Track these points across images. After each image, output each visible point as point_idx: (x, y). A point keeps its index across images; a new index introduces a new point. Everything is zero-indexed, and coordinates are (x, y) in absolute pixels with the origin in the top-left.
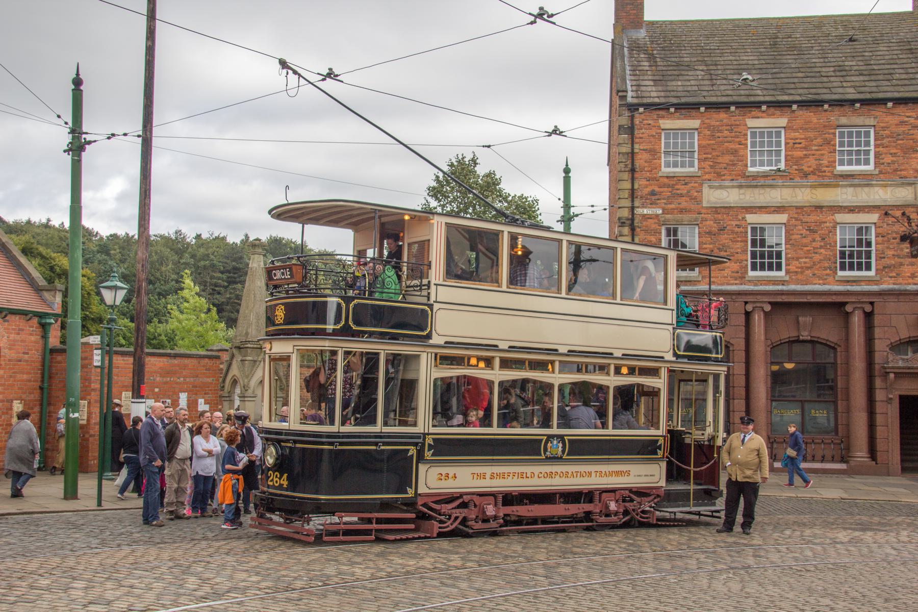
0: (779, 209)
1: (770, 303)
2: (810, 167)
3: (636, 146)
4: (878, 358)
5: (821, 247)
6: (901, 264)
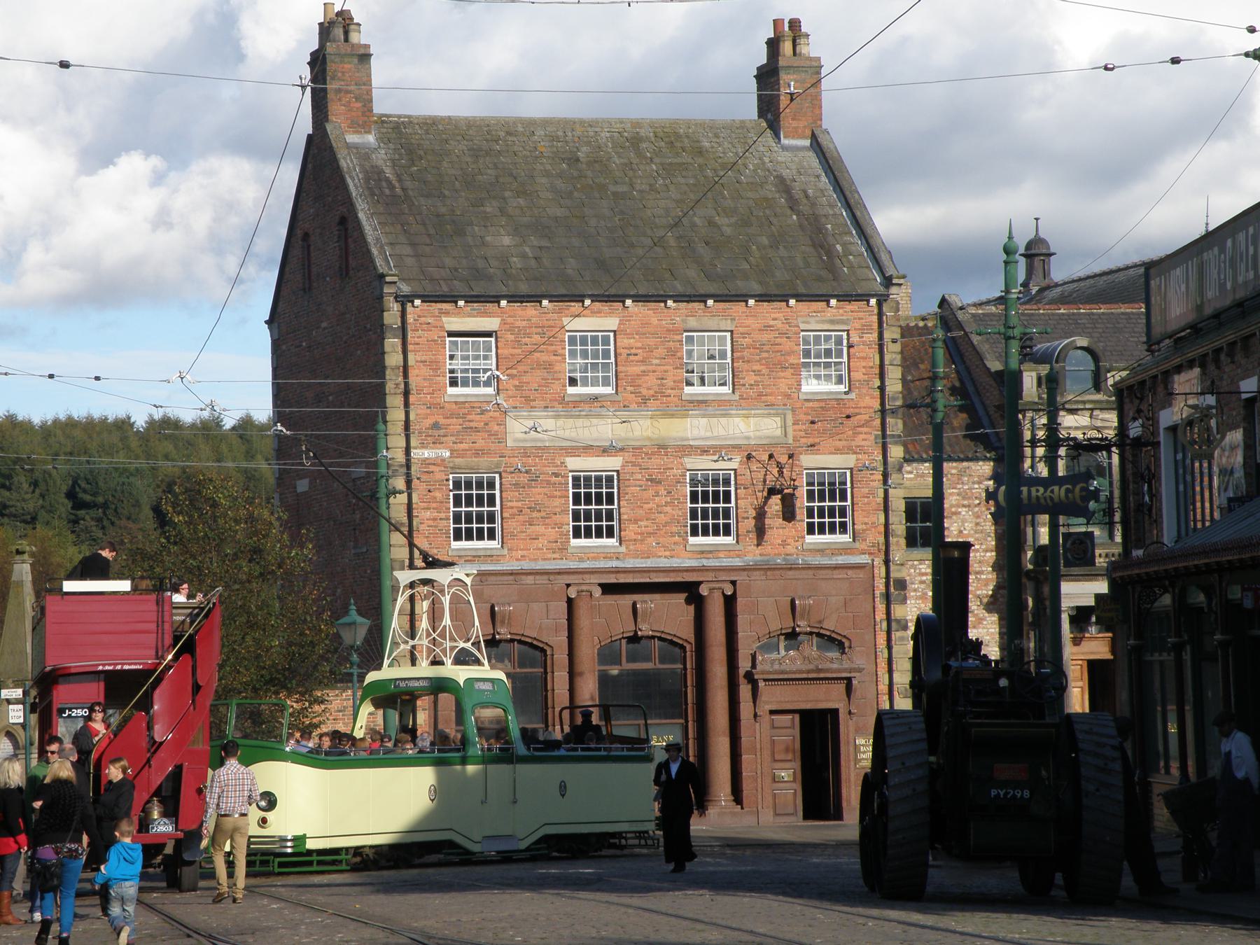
1: (600, 585)
2: (649, 389)
3: (411, 357)
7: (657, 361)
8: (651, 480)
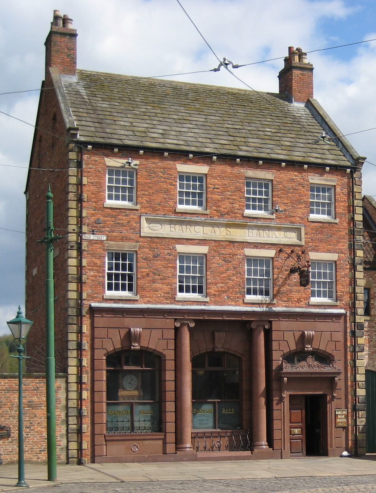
0: (202, 242)
1: (194, 320)
4: (275, 366)
5: (234, 275)
6: (291, 291)
7: (230, 193)
8: (225, 261)
